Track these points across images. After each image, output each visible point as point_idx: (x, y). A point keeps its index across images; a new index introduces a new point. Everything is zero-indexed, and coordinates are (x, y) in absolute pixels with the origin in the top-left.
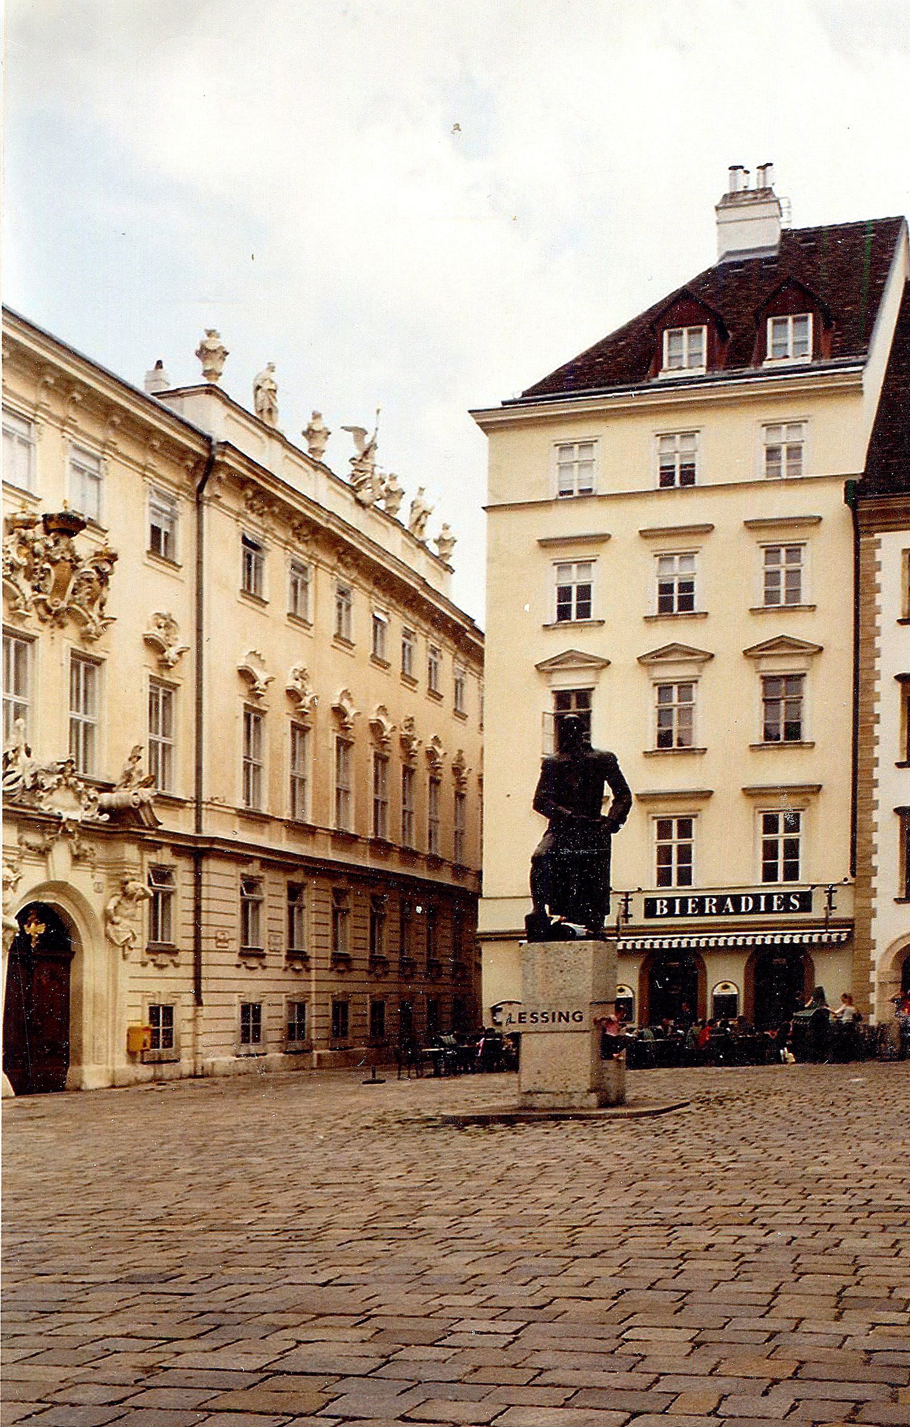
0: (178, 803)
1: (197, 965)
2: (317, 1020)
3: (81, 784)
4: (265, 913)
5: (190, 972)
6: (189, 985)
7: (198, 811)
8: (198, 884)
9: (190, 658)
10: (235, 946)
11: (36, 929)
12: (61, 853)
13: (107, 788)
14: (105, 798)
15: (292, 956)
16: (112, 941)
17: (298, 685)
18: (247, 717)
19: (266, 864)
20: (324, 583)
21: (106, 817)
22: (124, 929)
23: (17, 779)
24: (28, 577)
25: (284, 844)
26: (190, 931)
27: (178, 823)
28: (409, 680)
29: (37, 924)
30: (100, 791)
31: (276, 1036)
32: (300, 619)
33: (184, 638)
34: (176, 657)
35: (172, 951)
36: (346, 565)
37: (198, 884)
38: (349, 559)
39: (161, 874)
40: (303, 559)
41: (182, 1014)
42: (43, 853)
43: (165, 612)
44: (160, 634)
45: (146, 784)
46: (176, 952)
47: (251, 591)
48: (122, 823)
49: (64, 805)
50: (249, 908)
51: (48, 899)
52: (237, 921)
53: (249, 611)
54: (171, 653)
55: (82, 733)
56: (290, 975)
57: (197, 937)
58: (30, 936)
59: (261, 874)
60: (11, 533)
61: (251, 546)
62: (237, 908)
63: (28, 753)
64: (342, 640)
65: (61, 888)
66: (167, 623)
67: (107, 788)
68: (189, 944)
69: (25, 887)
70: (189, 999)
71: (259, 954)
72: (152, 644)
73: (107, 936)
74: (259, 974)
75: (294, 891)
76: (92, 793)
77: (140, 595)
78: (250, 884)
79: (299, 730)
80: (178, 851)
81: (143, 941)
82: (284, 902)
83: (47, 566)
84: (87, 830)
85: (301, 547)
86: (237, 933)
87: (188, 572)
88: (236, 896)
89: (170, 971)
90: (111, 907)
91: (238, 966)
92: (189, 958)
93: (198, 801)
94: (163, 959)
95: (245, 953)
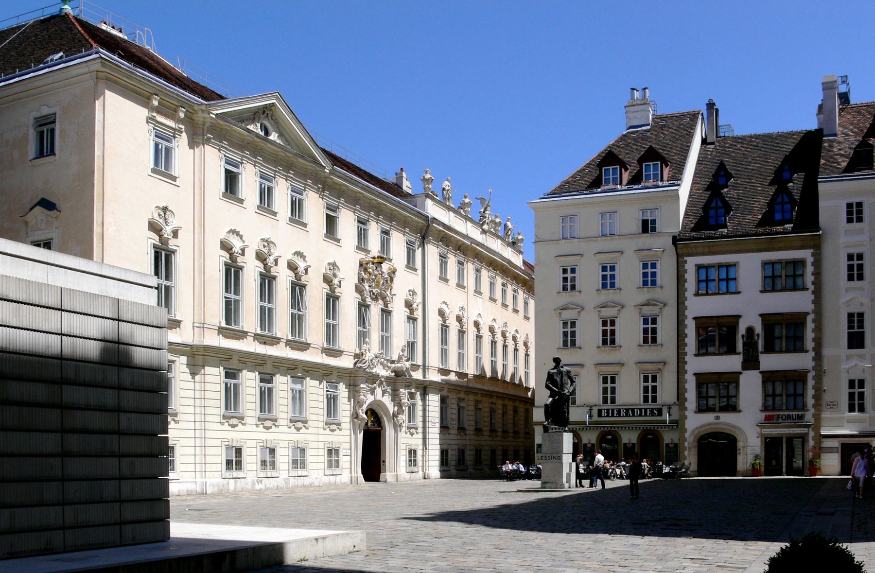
1: (424, 433)
2: (469, 457)
5: (420, 435)
6: (420, 441)
9: (420, 307)
12: (379, 391)
13: (393, 362)
20: (470, 268)
27: (417, 375)
28: (505, 306)
31: (453, 463)
33: (419, 299)
40: (462, 259)
41: (419, 453)
45: (408, 360)
53: (442, 284)
55: (385, 342)
56: (459, 437)
57: (424, 422)
64: (478, 292)
66: (413, 292)
70: (421, 447)
76: (389, 364)
77: (405, 283)
80: (417, 388)
87: (420, 272)
92: (420, 430)
93: (424, 366)
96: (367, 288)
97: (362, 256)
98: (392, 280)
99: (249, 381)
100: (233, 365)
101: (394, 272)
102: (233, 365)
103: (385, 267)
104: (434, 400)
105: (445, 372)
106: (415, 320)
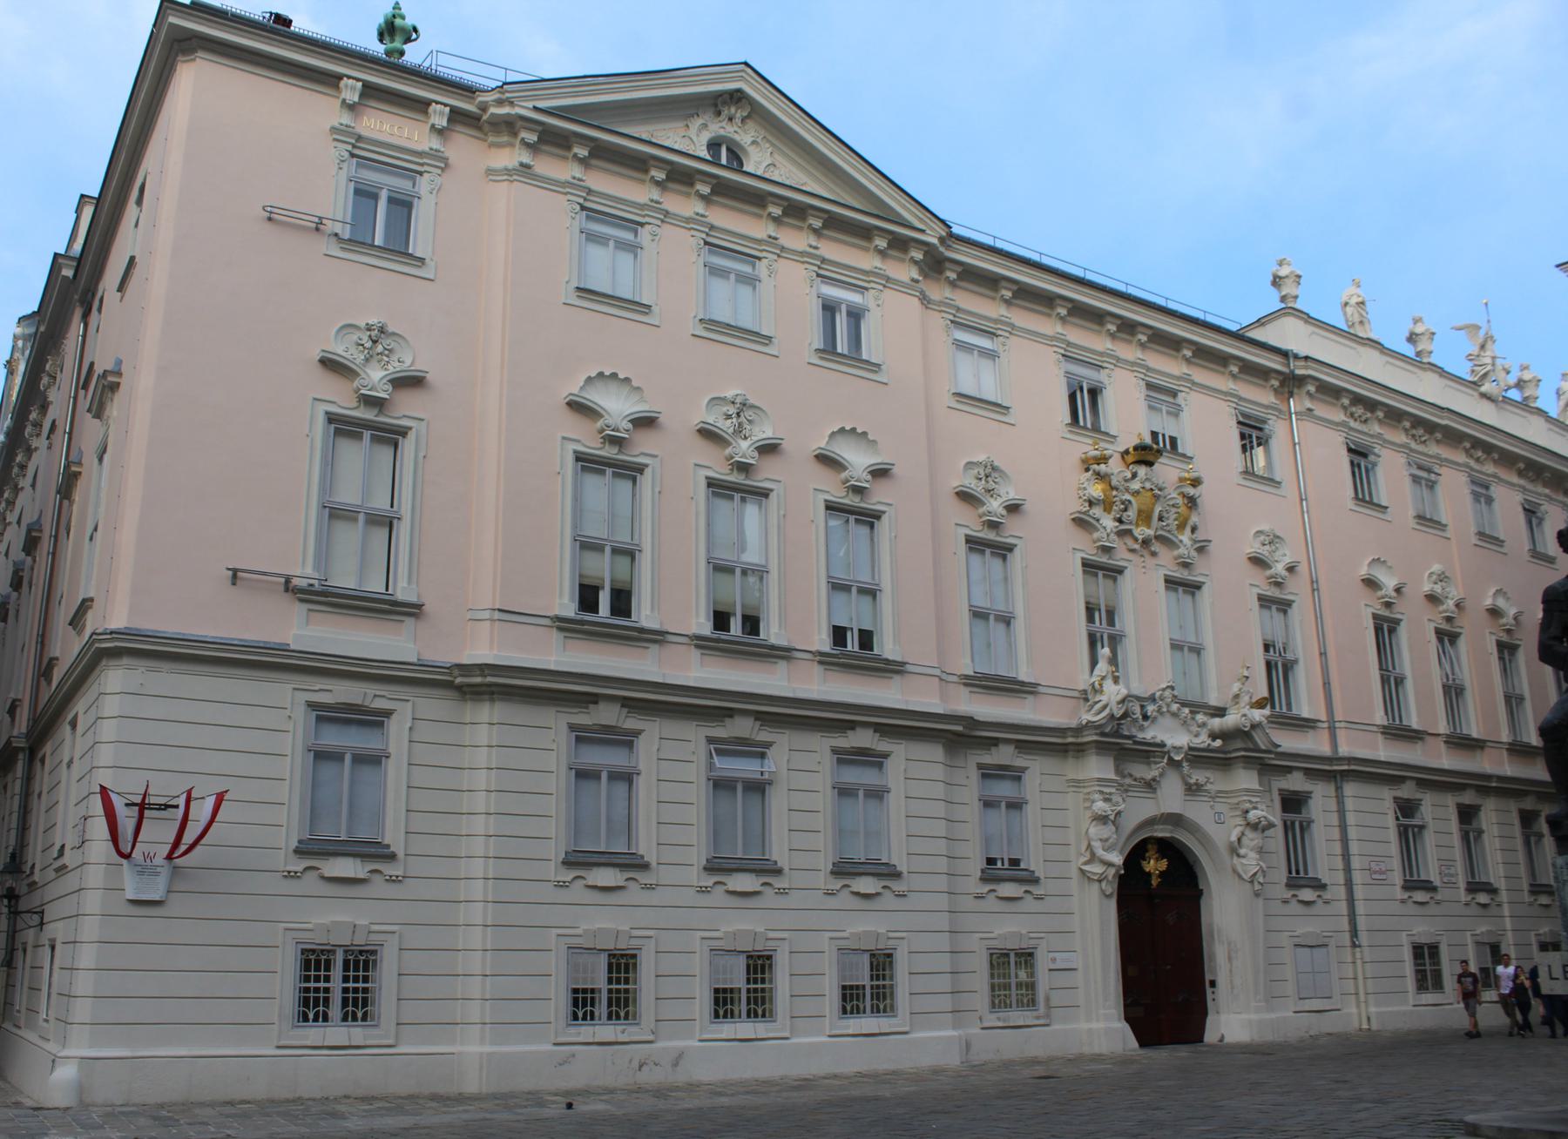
0: (1306, 724)
3: (1187, 710)
4: (1429, 839)
5: (1343, 907)
7: (1332, 730)
8: (1342, 812)
10: (1397, 878)
11: (1154, 865)
13: (1220, 712)
14: (1216, 723)
15: (1474, 887)
16: (1240, 876)
17: (1438, 588)
18: (1378, 630)
19: (1421, 783)
21: (1218, 743)
22: (1250, 862)
23: (1105, 707)
24: (1108, 509)
25: (1446, 760)
26: (1339, 863)
29: (1157, 860)
30: (1213, 716)
32: (1431, 520)
34: (1284, 573)
35: (1319, 886)
36: (1477, 460)
37: (1342, 812)
38: (1480, 454)
39: (1293, 803)
42: (1151, 786)
43: (1265, 527)
44: (1264, 551)
45: (1260, 704)
46: (1323, 887)
47: (1364, 497)
48: (1234, 750)
49: (1174, 736)
50: (1409, 835)
51: (1161, 832)
52: (1394, 848)
54: (1279, 568)
58: (1149, 874)
59: (1418, 796)
60: (1087, 470)
61: (1359, 454)
62: (1392, 835)
63: (1116, 680)
65: (1176, 820)
66: (1274, 540)
67: (1220, 712)
68: (1340, 878)
69: (1130, 823)
71: (1428, 886)
72: (1258, 561)
73: (1235, 871)
74: (1432, 909)
75: (1467, 815)
76: (1200, 718)
77: (1235, 515)
78: (1406, 808)
79: (1447, 637)
81: (1281, 875)
82: (1454, 825)
83: (1127, 497)
84: (1197, 757)
85: (1420, 448)
86: (1396, 863)
88: (1390, 821)
89: (1319, 908)
90: (1234, 838)
91: (1403, 901)
92: (1342, 892)
94: (1307, 894)
95: (1410, 886)
96: (1108, 522)
97: (1085, 446)
98: (1192, 502)
99: (672, 762)
100: (608, 718)
101: (1196, 482)
102: (608, 718)
103: (1167, 472)
104: (1371, 811)
105: (1399, 732)
106: (1284, 606)
